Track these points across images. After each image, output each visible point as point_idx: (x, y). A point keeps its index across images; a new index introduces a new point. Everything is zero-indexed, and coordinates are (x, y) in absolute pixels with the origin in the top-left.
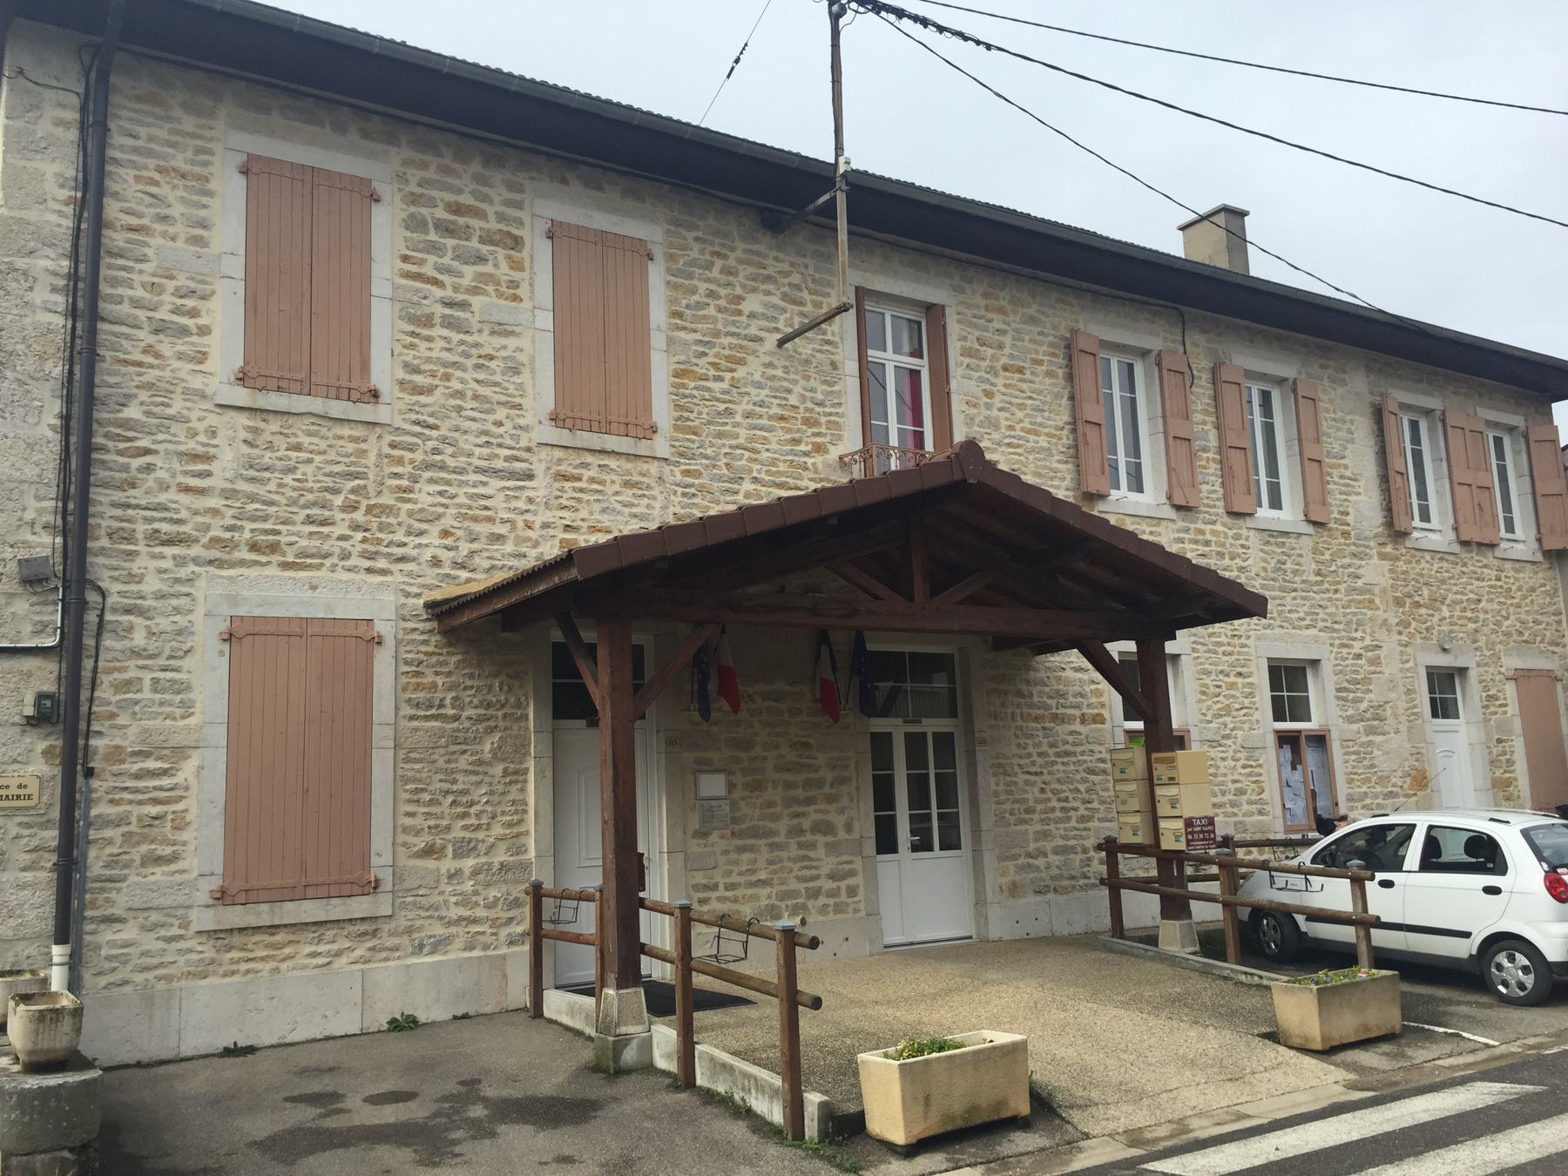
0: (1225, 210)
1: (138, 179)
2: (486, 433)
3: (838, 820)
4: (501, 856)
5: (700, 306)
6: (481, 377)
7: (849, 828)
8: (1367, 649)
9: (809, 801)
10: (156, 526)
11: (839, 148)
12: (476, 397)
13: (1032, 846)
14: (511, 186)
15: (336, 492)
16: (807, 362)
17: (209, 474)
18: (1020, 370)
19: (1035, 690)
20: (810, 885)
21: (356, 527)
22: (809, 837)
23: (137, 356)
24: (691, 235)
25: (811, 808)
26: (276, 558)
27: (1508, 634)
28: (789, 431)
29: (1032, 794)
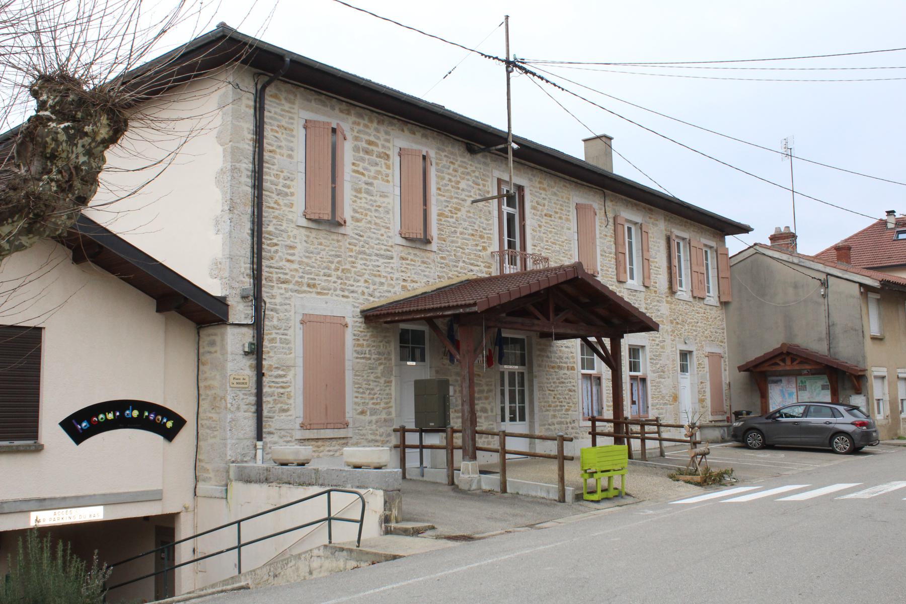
0: (605, 136)
1: (272, 130)
2: (378, 239)
3: (488, 407)
5: (446, 185)
6: (377, 215)
7: (492, 411)
8: (660, 342)
10: (280, 275)
11: (509, 127)
12: (376, 224)
13: (550, 421)
14: (387, 133)
15: (332, 262)
16: (481, 210)
17: (293, 255)
18: (550, 216)
21: (338, 278)
23: (272, 205)
24: (443, 154)
26: (314, 290)
27: (706, 337)
28: (474, 240)
29: (551, 399)
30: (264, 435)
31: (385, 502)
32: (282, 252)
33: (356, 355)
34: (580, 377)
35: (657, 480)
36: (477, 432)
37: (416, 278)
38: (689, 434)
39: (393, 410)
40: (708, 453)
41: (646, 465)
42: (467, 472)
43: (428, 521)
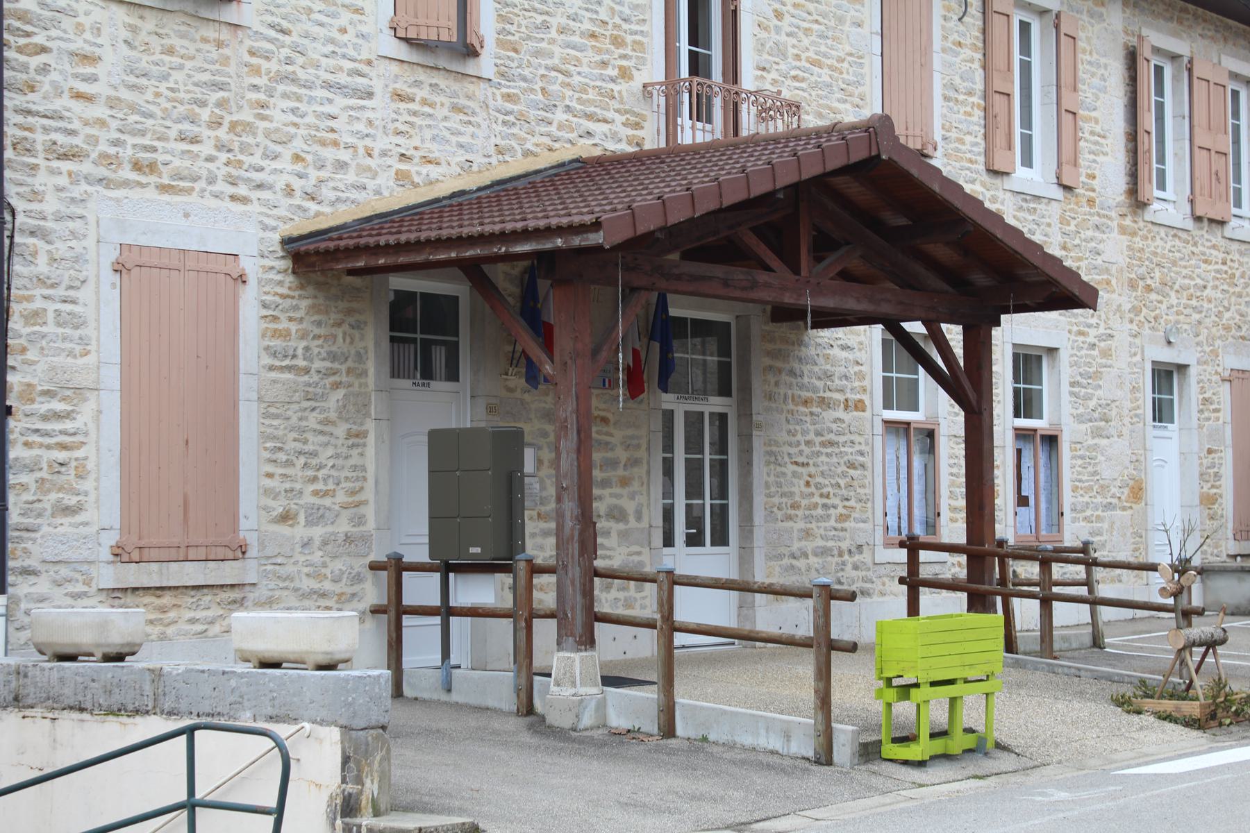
2: (332, 41)
3: (630, 507)
4: (343, 527)
7: (639, 518)
8: (1100, 338)
13: (796, 546)
15: (203, 104)
17: (93, 79)
19: (806, 369)
21: (220, 147)
26: (153, 179)
27: (1227, 328)
28: (599, 51)
29: (799, 487)
30: (10, 579)
31: (346, 760)
32: (62, 72)
33: (268, 361)
34: (879, 428)
35: (1081, 709)
36: (597, 573)
37: (435, 150)
38: (1171, 587)
39: (369, 512)
40: (1223, 642)
41: (1052, 670)
42: (569, 679)
43: (461, 811)
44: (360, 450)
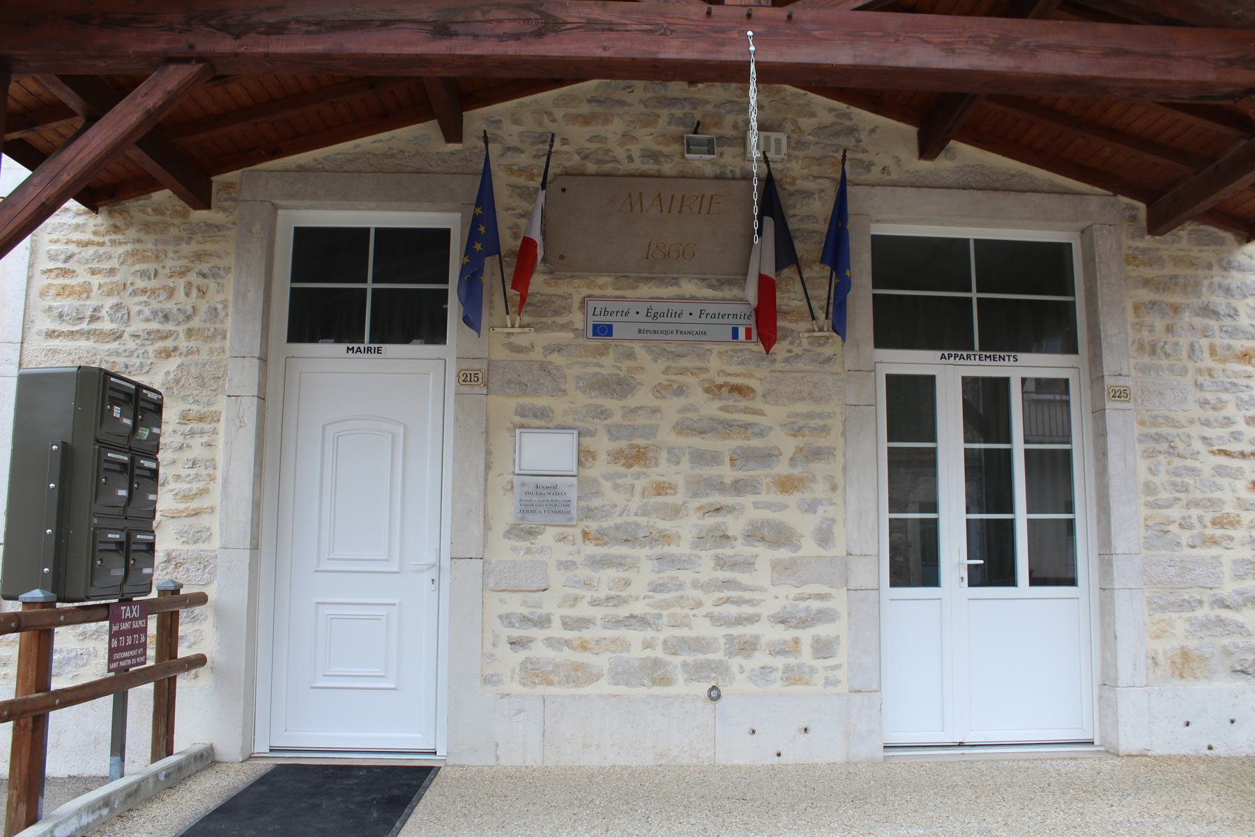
3: (805, 525)
7: (824, 537)
9: (739, 487)
20: (736, 631)
22: (741, 549)
25: (748, 500)
44: (205, 439)
